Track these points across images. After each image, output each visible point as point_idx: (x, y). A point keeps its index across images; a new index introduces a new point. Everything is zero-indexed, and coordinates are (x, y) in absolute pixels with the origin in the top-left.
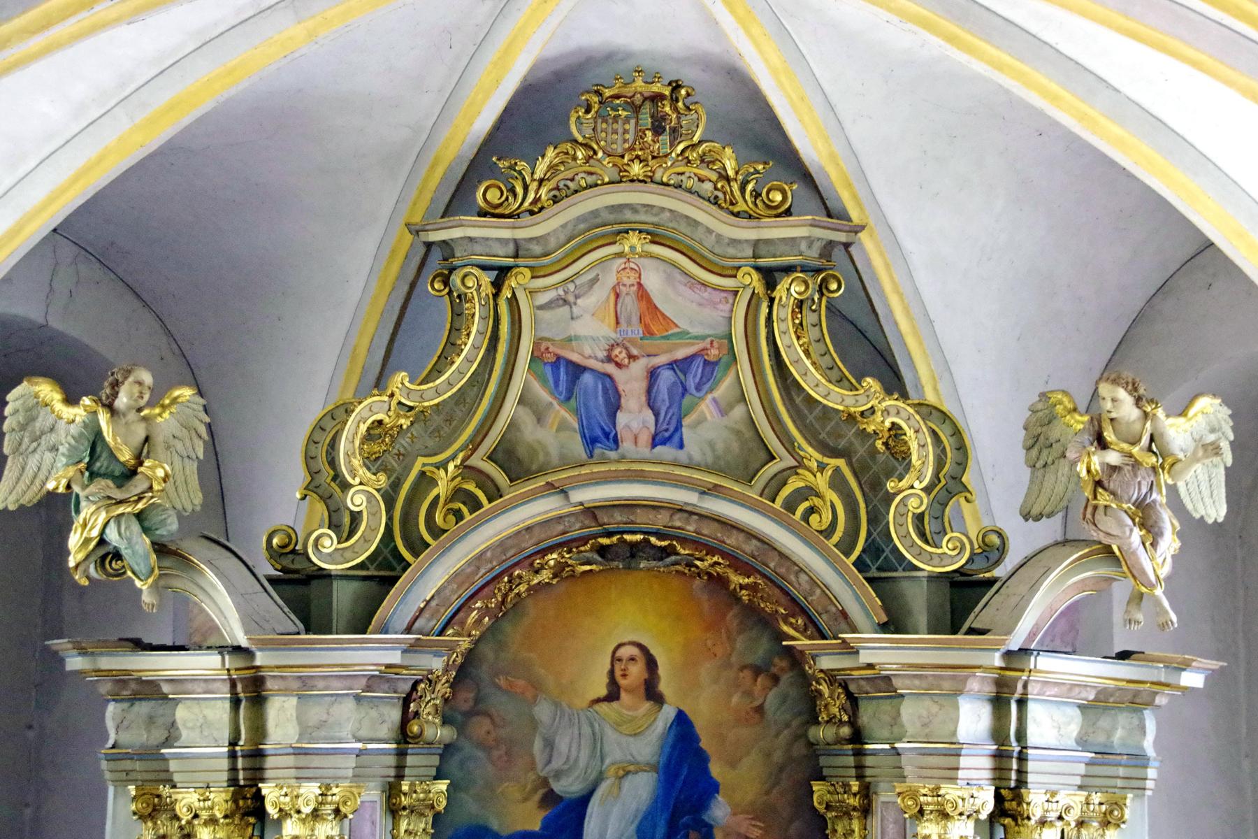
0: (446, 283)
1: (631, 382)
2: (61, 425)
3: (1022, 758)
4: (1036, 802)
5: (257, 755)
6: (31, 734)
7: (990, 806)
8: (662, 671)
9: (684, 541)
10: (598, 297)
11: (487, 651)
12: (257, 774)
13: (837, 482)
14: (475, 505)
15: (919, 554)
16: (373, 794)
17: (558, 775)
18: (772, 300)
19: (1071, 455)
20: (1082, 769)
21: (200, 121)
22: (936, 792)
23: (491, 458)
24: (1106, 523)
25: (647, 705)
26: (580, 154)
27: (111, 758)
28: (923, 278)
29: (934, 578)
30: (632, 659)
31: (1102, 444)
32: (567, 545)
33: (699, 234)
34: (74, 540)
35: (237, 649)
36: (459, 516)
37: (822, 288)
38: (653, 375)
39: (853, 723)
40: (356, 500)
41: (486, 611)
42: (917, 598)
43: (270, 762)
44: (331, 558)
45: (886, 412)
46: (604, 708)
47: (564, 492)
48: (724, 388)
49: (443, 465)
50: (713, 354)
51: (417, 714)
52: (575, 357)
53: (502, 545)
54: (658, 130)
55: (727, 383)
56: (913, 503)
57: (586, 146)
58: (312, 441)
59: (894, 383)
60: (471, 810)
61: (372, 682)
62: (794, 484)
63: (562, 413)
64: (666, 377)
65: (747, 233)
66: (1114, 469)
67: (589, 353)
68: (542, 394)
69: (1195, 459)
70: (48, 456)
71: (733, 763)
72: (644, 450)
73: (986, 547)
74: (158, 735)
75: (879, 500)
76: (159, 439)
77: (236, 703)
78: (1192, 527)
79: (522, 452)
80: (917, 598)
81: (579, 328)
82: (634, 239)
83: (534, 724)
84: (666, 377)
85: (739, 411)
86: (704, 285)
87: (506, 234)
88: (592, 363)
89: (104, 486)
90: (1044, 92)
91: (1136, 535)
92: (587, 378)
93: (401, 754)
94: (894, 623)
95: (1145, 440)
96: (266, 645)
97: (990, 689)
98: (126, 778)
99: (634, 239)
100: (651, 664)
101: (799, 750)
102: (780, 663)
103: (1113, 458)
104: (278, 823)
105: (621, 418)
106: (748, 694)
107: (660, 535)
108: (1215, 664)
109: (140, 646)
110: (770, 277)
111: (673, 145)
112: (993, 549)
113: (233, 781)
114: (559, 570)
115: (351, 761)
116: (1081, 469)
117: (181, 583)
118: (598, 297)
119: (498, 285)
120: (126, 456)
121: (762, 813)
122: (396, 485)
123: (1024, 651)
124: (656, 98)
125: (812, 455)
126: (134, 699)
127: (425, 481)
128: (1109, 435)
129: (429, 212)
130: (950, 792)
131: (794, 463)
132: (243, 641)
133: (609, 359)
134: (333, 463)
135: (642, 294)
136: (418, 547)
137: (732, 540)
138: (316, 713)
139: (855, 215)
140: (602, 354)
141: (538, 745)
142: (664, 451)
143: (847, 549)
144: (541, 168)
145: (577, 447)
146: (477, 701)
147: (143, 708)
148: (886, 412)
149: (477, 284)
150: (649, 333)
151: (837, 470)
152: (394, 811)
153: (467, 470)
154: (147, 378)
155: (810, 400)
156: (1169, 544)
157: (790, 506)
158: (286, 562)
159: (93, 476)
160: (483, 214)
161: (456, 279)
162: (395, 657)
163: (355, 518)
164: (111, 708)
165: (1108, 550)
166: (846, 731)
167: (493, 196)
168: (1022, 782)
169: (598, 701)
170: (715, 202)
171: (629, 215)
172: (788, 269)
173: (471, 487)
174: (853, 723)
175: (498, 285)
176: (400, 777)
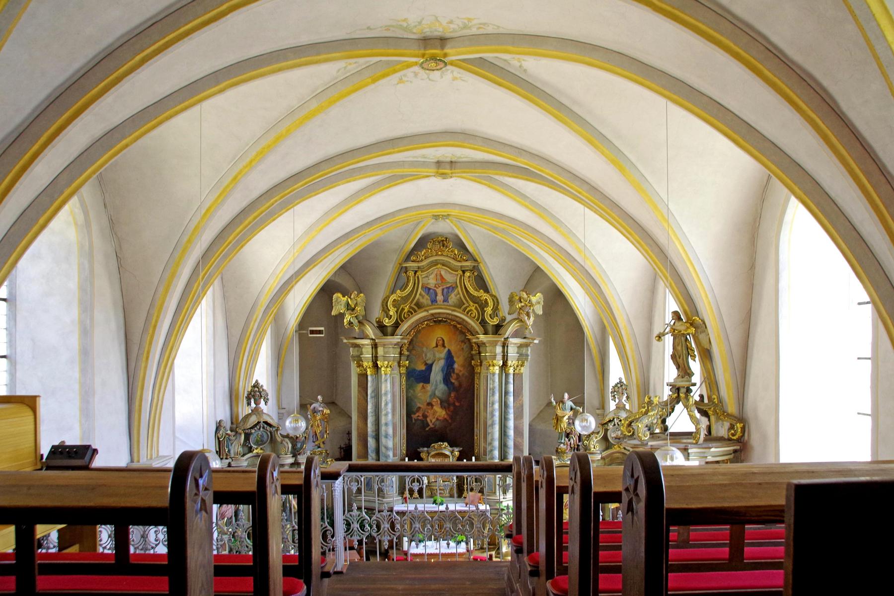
0: (406, 273)
1: (439, 291)
2: (342, 301)
3: (507, 356)
4: (509, 363)
5: (376, 357)
6: (334, 353)
7: (502, 364)
8: (446, 342)
9: (449, 319)
10: (432, 276)
11: (415, 339)
12: (377, 360)
13: (476, 308)
14: (412, 314)
15: (490, 321)
16: (396, 364)
17: (427, 360)
18: (464, 276)
19: (516, 304)
20: (517, 357)
21: (365, 247)
22: (492, 362)
23: (415, 305)
24: (522, 316)
25: (442, 348)
26: (430, 251)
27: (351, 357)
28: (491, 270)
29: (493, 325)
30: (440, 340)
31: (521, 302)
32: (428, 320)
33: (451, 264)
34: (345, 321)
35: (372, 339)
36: (409, 315)
37: (473, 273)
38: (443, 290)
39: (479, 350)
40: (391, 313)
41: (414, 332)
42: (490, 329)
43: (379, 358)
44: (387, 323)
45: (484, 296)
46: (435, 348)
47: (428, 311)
48: (456, 292)
49: (406, 306)
50: (454, 286)
51: (403, 350)
52: (429, 287)
53: (417, 320)
54: (443, 246)
55: (456, 291)
56: (489, 312)
57: (431, 249)
58: (383, 302)
59: (487, 290)
60: (412, 366)
61: (395, 345)
62: (468, 309)
63: (427, 297)
64: (445, 290)
65: (459, 264)
66: (523, 306)
67: (432, 286)
68: (423, 293)
69: (536, 304)
70: (340, 306)
71: (458, 358)
72: (442, 303)
73: (502, 319)
74: (359, 353)
75: (483, 312)
76: (358, 303)
77: (372, 348)
78: (536, 316)
79: (420, 304)
80: (490, 329)
81: (430, 281)
82: (439, 266)
83: (423, 352)
84: (445, 290)
85: (458, 296)
86: (452, 273)
87: (416, 265)
88: (432, 288)
89: (349, 312)
90: (510, 242)
91: (526, 317)
92: (431, 291)
93: (400, 357)
94: (486, 333)
95: (528, 301)
96: (378, 339)
97: (502, 344)
98: (354, 360)
99: (439, 266)
100: (443, 341)
101: (470, 356)
102: (466, 340)
103: (523, 304)
104: (381, 368)
105: (437, 297)
106: (461, 346)
107: (445, 318)
108: (540, 339)
109: (355, 338)
110: (464, 272)
111: (446, 249)
112: (503, 320)
113: (373, 361)
114: (427, 324)
115: (392, 358)
116: (517, 307)
117: (363, 328)
118: (432, 276)
119: (415, 274)
120: (353, 306)
121: (463, 366)
122: (398, 310)
123: (508, 338)
124: (443, 241)
125: (472, 304)
126: (355, 347)
127: (403, 309)
128: (522, 300)
129: (402, 261)
130: (495, 362)
131: (468, 305)
132: (374, 338)
133: (435, 287)
134: (387, 306)
135: (441, 276)
136: (402, 321)
137: (457, 319)
138: (386, 350)
139: (478, 260)
140: (434, 286)
141: (424, 355)
142: (445, 303)
143: (478, 320)
144: (423, 253)
145: (430, 303)
146: (413, 348)
147: (356, 349)
148: (484, 296)
149: (411, 274)
150: (442, 282)
151: (476, 307)
152: (399, 366)
153: (410, 307)
154: (356, 293)
155: (471, 294)
156: (532, 319)
157: (468, 313)
158: (379, 323)
159: (348, 310)
160: (412, 261)
161: (408, 273)
162: (399, 340)
163: (391, 316)
164: (351, 349)
165: (522, 320)
166: (477, 352)
167: (414, 258)
168: (507, 360)
169: (434, 348)
170: (454, 259)
171: (438, 261)
172: (467, 270)
173: (411, 310)
174: (479, 350)
175: (415, 274)
176: (400, 360)
